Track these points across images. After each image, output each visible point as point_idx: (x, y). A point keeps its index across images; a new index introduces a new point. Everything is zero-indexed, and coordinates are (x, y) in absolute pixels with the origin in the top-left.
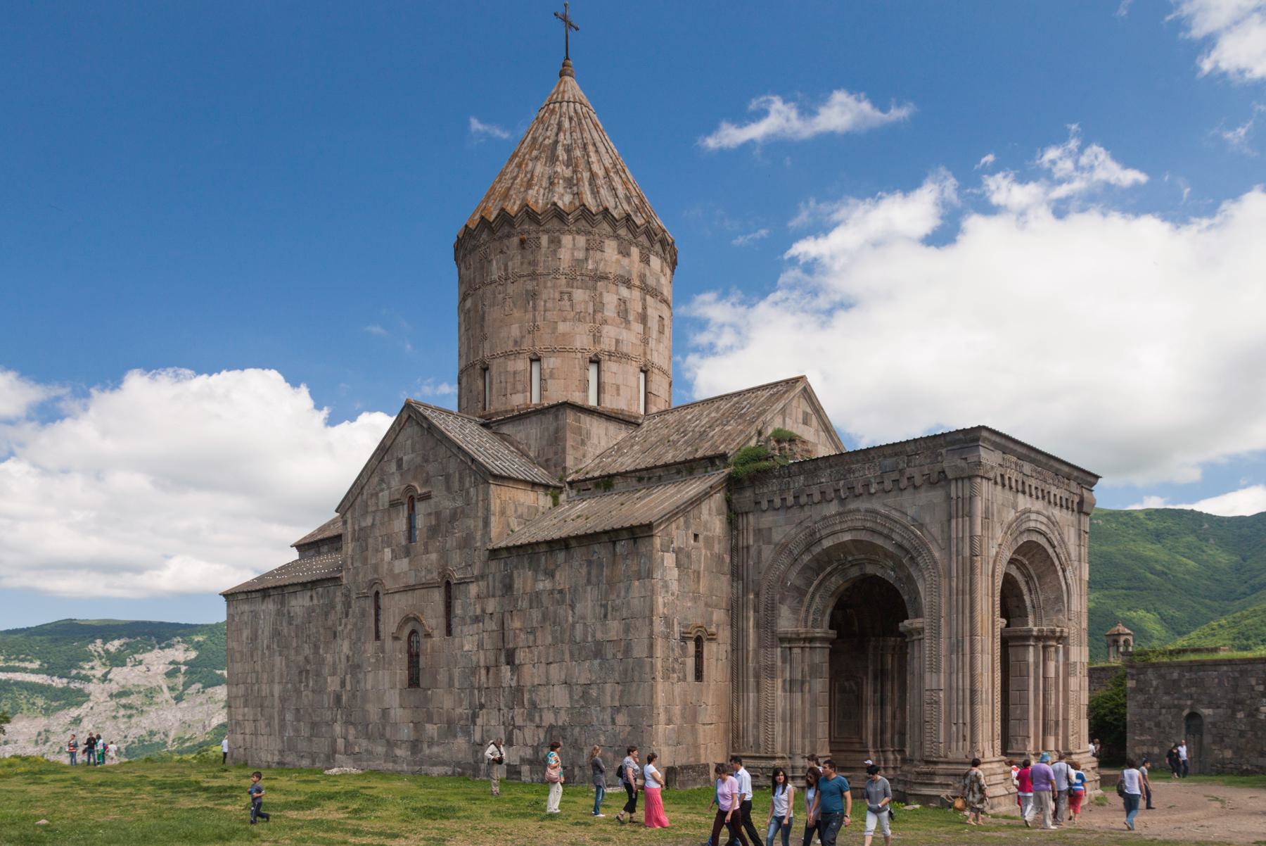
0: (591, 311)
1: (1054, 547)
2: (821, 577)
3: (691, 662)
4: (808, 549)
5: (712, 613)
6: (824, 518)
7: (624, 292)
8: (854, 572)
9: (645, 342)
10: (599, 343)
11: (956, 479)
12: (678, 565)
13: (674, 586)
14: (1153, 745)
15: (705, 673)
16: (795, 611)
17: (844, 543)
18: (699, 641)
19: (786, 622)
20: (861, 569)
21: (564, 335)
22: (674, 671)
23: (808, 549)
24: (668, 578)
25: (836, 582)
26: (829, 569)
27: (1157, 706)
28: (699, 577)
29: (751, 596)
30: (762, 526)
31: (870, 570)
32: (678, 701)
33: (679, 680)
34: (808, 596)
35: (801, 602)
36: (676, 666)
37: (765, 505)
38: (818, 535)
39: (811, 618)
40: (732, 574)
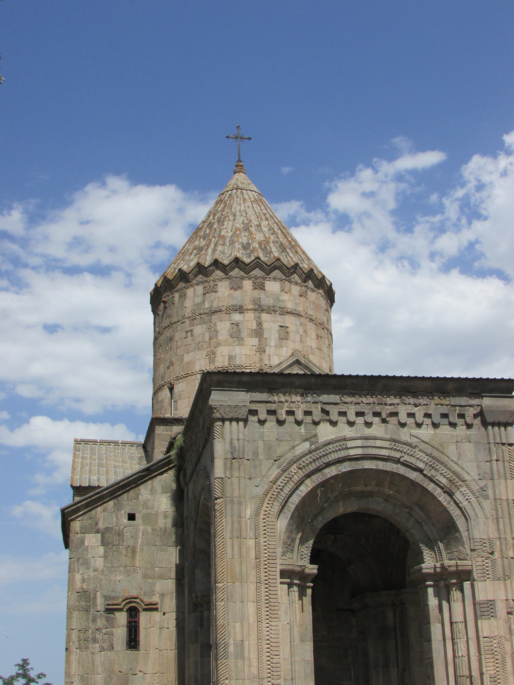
0: (207, 339)
1: (421, 471)
3: (121, 632)
5: (154, 584)
7: (237, 317)
9: (261, 350)
10: (214, 362)
12: (104, 543)
13: (99, 563)
18: (133, 613)
21: (188, 363)
22: (95, 641)
24: (90, 556)
28: (134, 551)
32: (100, 670)
33: (102, 649)
36: (99, 636)
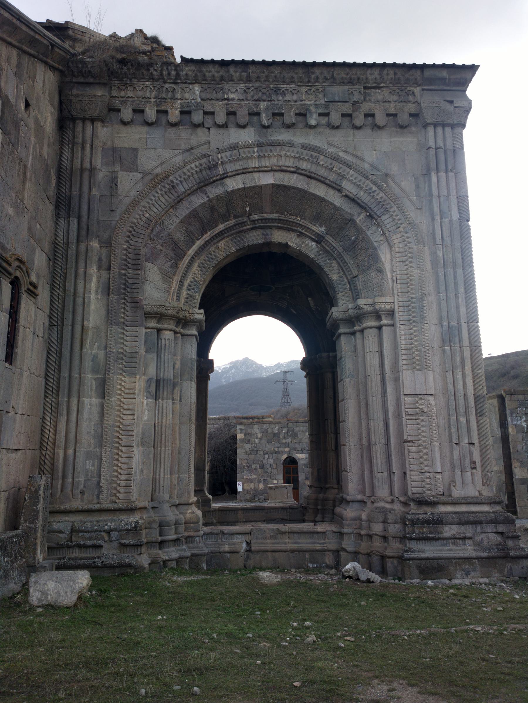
2: (207, 236)
4: (201, 187)
6: (234, 147)
8: (255, 238)
11: (435, 125)
14: (259, 481)
15: (18, 351)
16: (167, 277)
17: (258, 189)
19: (155, 290)
20: (266, 235)
23: (201, 187)
25: (225, 249)
26: (221, 227)
27: (261, 452)
29: (95, 244)
30: (118, 144)
31: (279, 237)
34: (186, 261)
35: (175, 266)
37: (127, 114)
38: (221, 170)
39: (184, 294)
40: (57, 206)
